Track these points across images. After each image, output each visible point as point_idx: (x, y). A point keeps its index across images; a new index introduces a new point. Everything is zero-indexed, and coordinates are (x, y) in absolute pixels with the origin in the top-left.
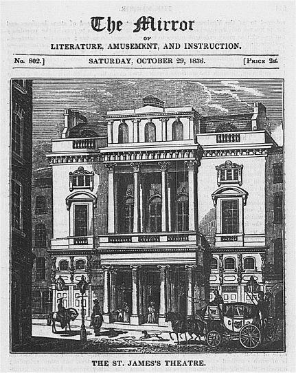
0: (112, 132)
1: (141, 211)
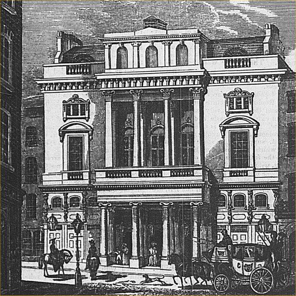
0: (169, 56)
1: (173, 145)
